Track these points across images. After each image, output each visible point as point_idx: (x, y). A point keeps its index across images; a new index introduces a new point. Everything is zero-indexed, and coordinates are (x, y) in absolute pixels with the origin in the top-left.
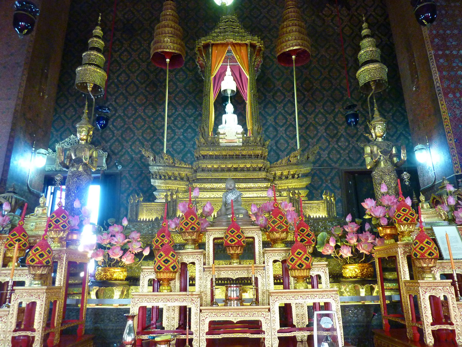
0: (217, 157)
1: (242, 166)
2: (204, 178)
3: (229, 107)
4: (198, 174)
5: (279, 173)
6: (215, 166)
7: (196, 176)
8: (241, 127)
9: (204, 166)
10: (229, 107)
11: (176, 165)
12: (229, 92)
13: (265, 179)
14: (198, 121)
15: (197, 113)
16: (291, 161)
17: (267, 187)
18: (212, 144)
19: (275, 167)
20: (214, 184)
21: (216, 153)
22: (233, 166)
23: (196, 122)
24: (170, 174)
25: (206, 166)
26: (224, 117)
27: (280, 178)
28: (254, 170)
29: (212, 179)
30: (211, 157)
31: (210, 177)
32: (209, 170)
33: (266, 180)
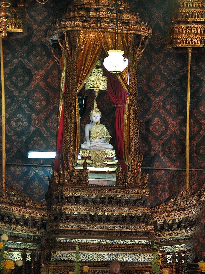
0: (85, 201)
1: (116, 214)
2: (69, 229)
3: (96, 115)
4: (62, 224)
5: (160, 221)
6: (82, 213)
7: (58, 226)
8: (111, 147)
9: (68, 212)
10: (96, 115)
11: (27, 205)
12: (97, 91)
13: (145, 233)
14: (17, 77)
15: (16, 61)
16: (177, 205)
17: (147, 245)
18: (79, 182)
19: (155, 213)
20: (81, 239)
21: (84, 195)
22: (104, 213)
23: (14, 78)
24: (18, 217)
25: (71, 212)
26: (88, 127)
27: (162, 228)
28: (132, 220)
29: (78, 231)
30: (77, 201)
31: (76, 229)
32: (76, 219)
33: (145, 234)
